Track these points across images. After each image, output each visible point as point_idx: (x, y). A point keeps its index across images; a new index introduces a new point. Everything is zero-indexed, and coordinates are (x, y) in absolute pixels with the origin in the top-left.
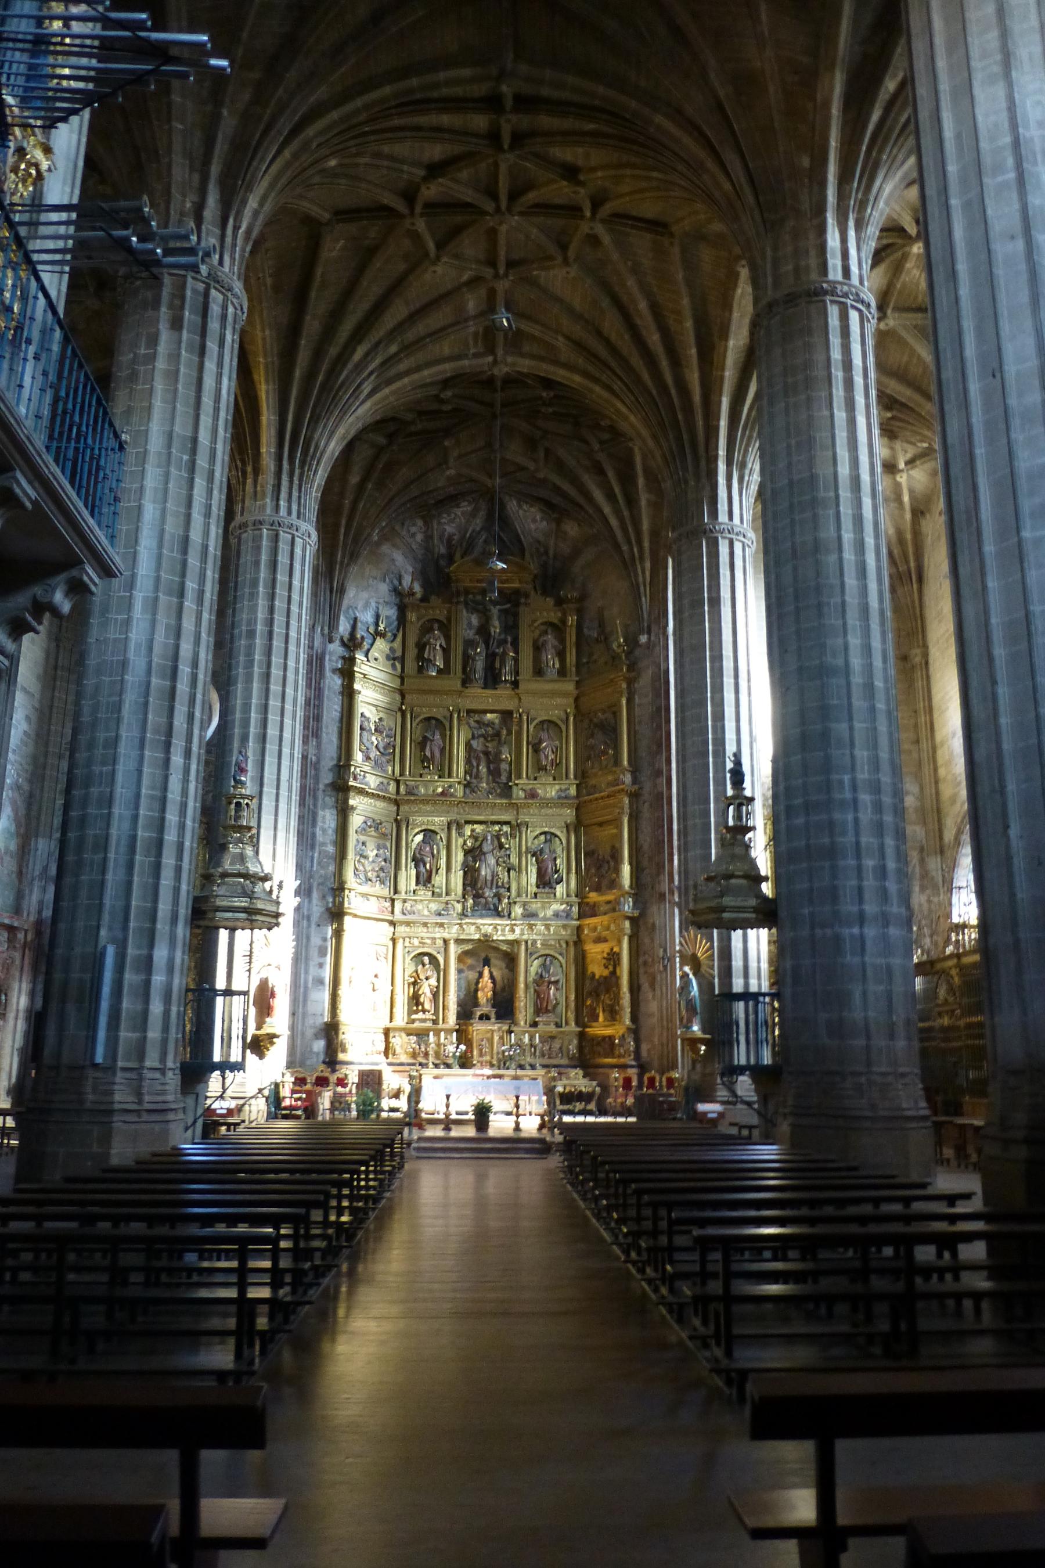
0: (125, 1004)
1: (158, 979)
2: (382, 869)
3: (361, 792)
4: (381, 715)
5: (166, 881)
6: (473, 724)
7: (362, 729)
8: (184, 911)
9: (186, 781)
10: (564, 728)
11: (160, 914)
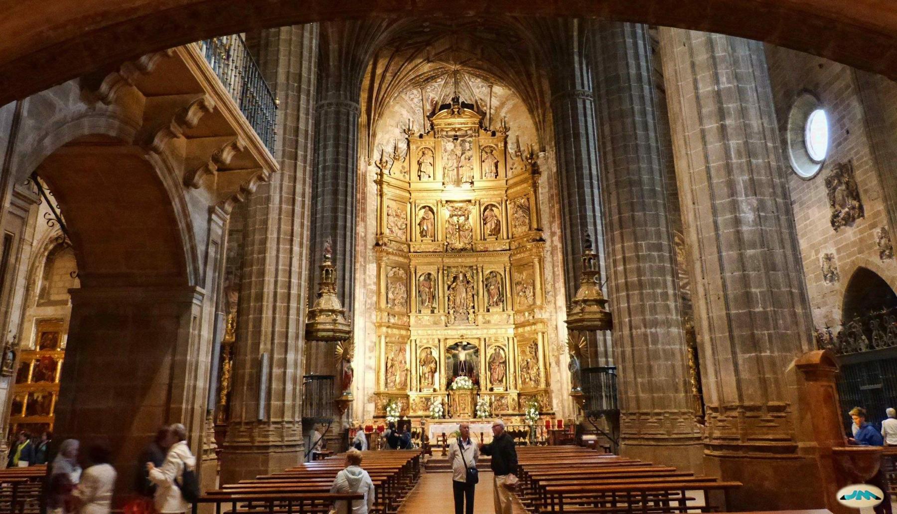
0: (274, 386)
1: (290, 371)
5: (293, 316)
8: (302, 333)
9: (301, 260)
11: (290, 335)
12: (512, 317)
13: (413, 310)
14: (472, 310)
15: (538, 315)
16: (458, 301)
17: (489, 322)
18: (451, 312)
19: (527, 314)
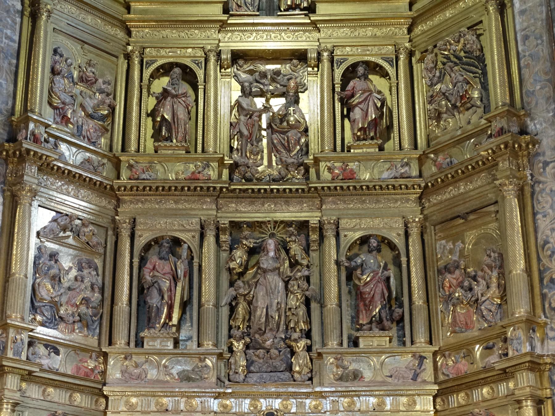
2: (86, 301)
3: (47, 168)
4: (90, 56)
6: (244, 76)
7: (54, 72)
10: (391, 71)
12: (428, 364)
13: (120, 341)
14: (302, 343)
15: (521, 345)
16: (260, 313)
17: (356, 376)
18: (239, 346)
19: (478, 349)
